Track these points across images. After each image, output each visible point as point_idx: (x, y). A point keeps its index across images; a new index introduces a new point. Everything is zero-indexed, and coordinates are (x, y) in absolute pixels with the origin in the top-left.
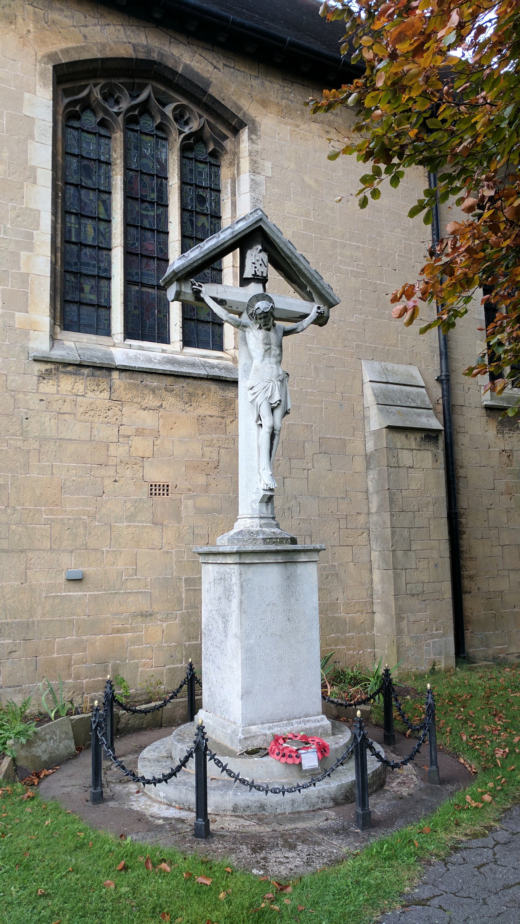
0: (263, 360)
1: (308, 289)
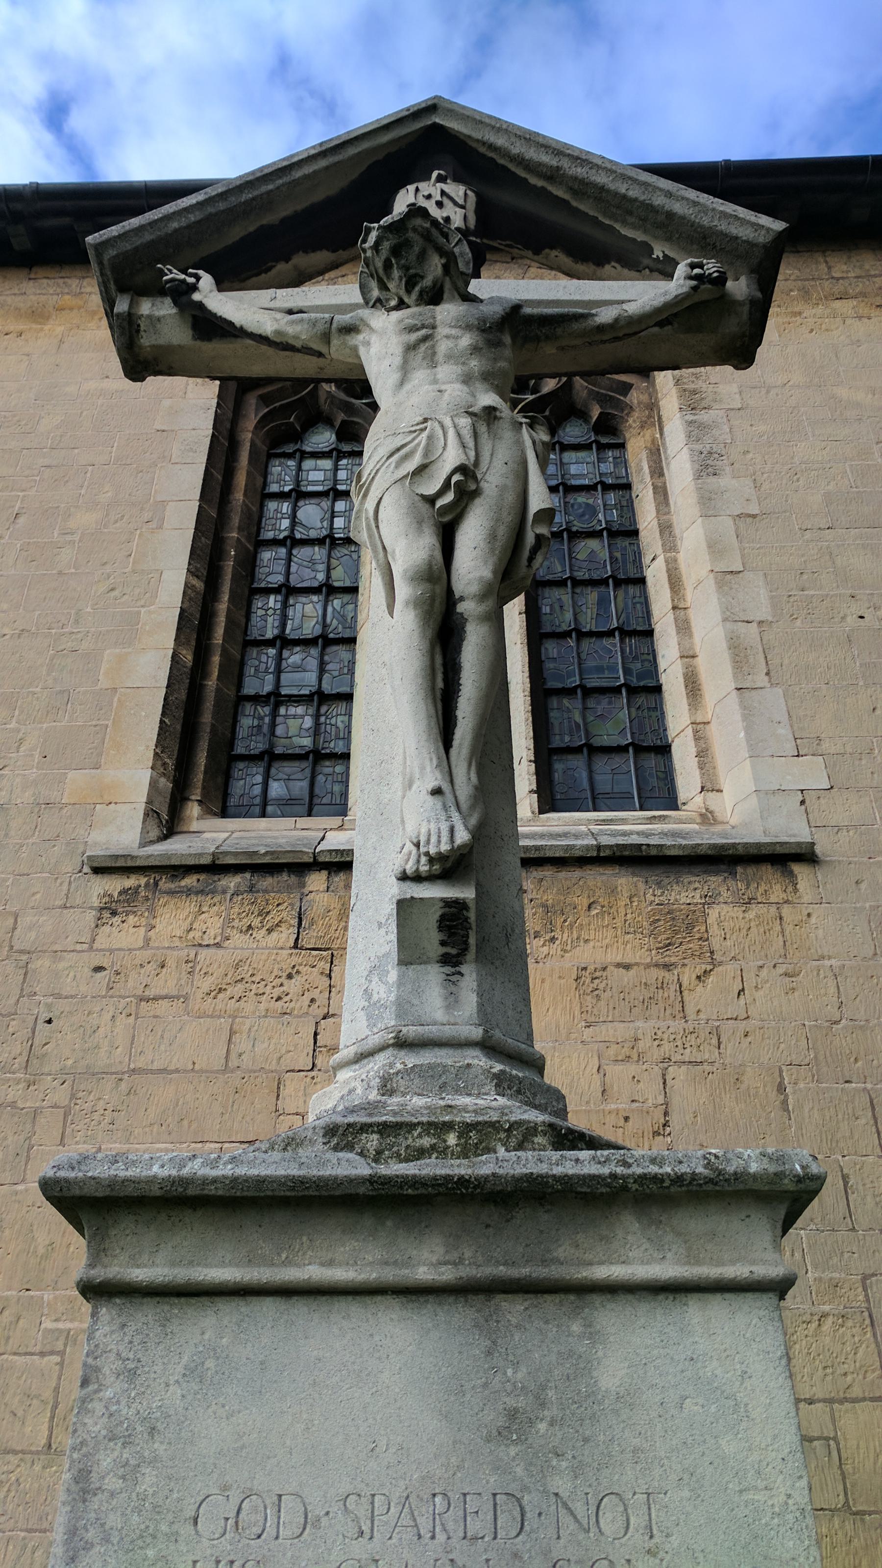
0: (402, 383)
1: (658, 253)
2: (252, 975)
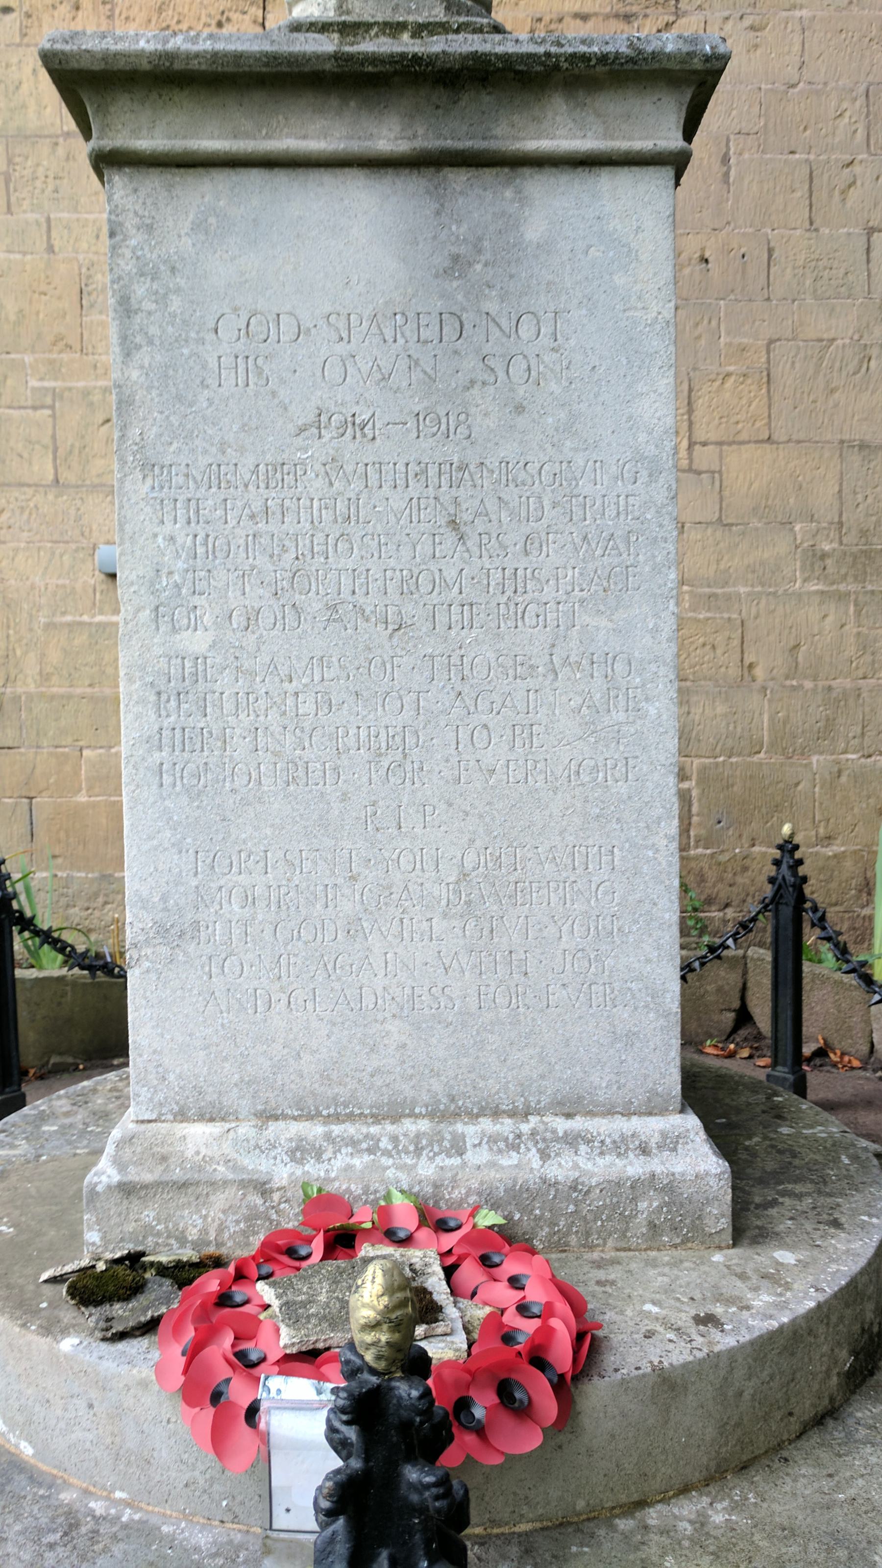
2: (179, 22)
